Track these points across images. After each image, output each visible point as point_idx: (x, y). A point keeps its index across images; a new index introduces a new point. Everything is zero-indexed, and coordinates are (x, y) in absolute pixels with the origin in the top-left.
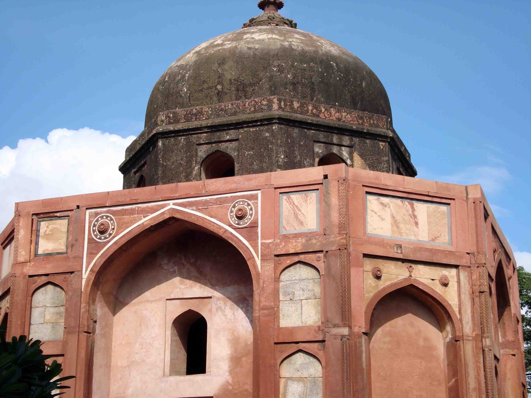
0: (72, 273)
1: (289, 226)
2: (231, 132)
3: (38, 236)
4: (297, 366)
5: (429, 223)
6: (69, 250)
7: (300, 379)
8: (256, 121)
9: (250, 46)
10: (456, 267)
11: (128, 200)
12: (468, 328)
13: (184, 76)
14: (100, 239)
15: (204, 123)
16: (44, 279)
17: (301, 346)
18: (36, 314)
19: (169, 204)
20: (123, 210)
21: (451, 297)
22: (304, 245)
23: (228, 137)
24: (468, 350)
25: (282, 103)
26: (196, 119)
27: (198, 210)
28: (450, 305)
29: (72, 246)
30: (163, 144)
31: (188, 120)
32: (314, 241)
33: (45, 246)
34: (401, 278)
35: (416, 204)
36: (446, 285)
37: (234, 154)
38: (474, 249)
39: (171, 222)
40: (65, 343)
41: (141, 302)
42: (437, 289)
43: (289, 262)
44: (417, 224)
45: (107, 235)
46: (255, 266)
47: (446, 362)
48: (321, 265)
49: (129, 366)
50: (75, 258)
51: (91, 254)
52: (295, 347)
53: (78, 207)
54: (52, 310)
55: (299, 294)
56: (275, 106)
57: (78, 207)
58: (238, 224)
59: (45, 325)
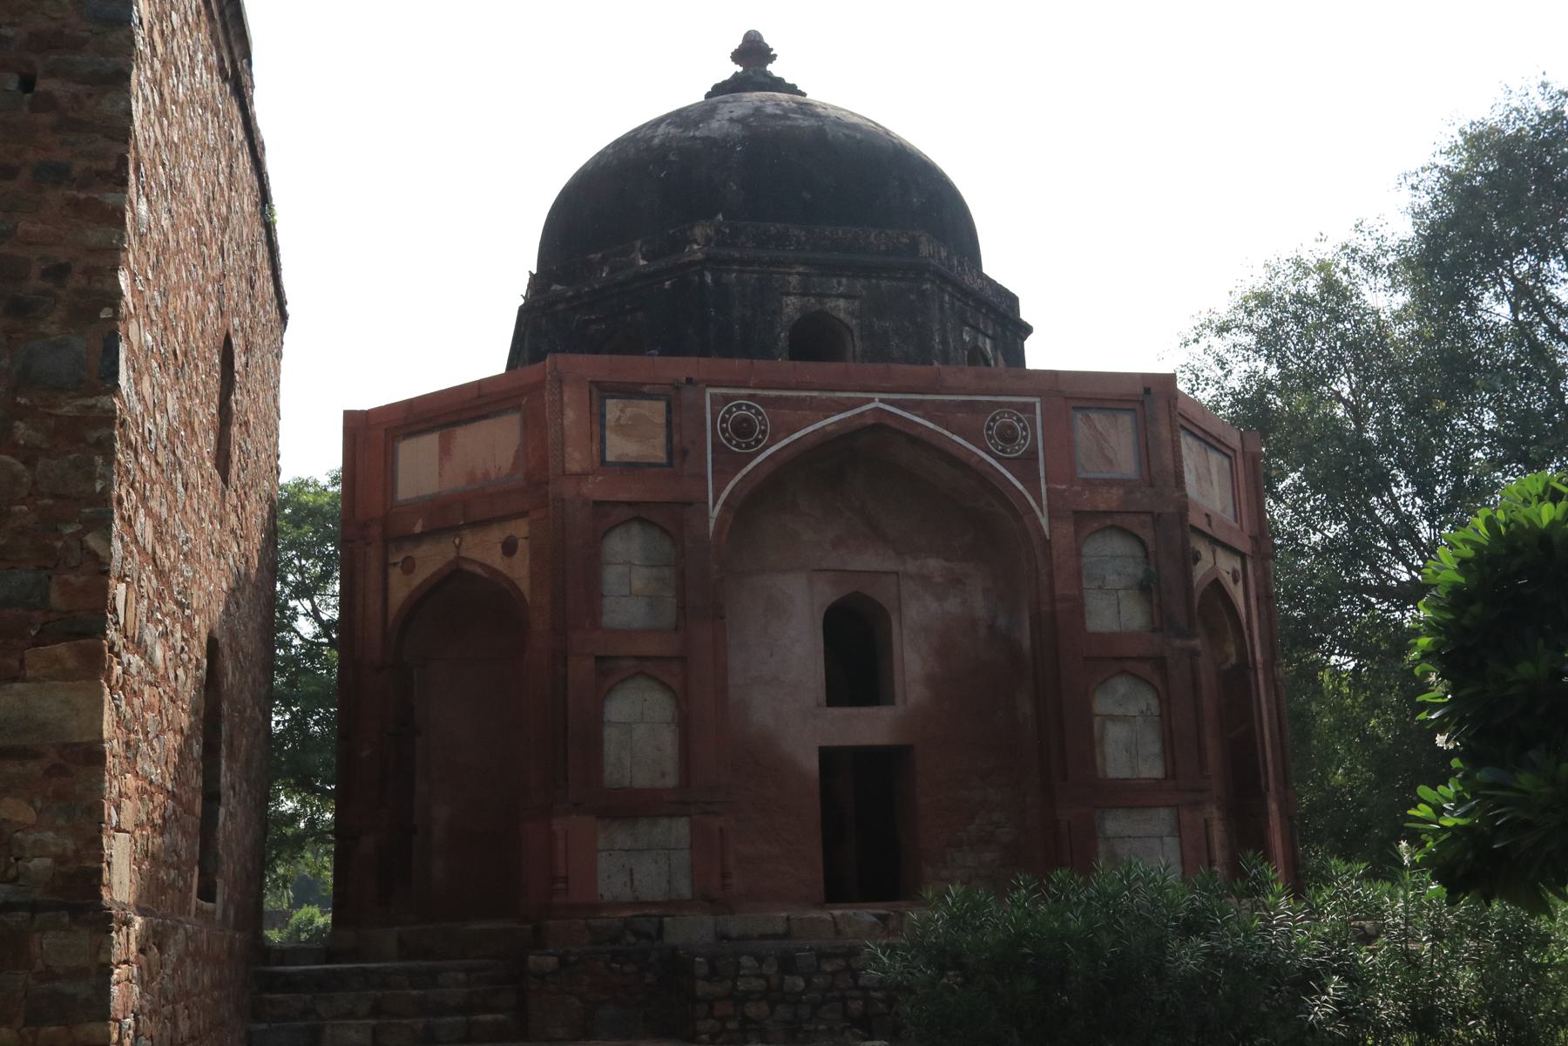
0: (690, 504)
1: (1090, 467)
3: (603, 426)
7: (1124, 719)
18: (612, 577)
19: (872, 400)
29: (685, 453)
33: (619, 447)
39: (880, 429)
46: (1040, 528)
48: (1147, 535)
51: (722, 475)
53: (689, 380)
57: (689, 380)
58: (1003, 451)
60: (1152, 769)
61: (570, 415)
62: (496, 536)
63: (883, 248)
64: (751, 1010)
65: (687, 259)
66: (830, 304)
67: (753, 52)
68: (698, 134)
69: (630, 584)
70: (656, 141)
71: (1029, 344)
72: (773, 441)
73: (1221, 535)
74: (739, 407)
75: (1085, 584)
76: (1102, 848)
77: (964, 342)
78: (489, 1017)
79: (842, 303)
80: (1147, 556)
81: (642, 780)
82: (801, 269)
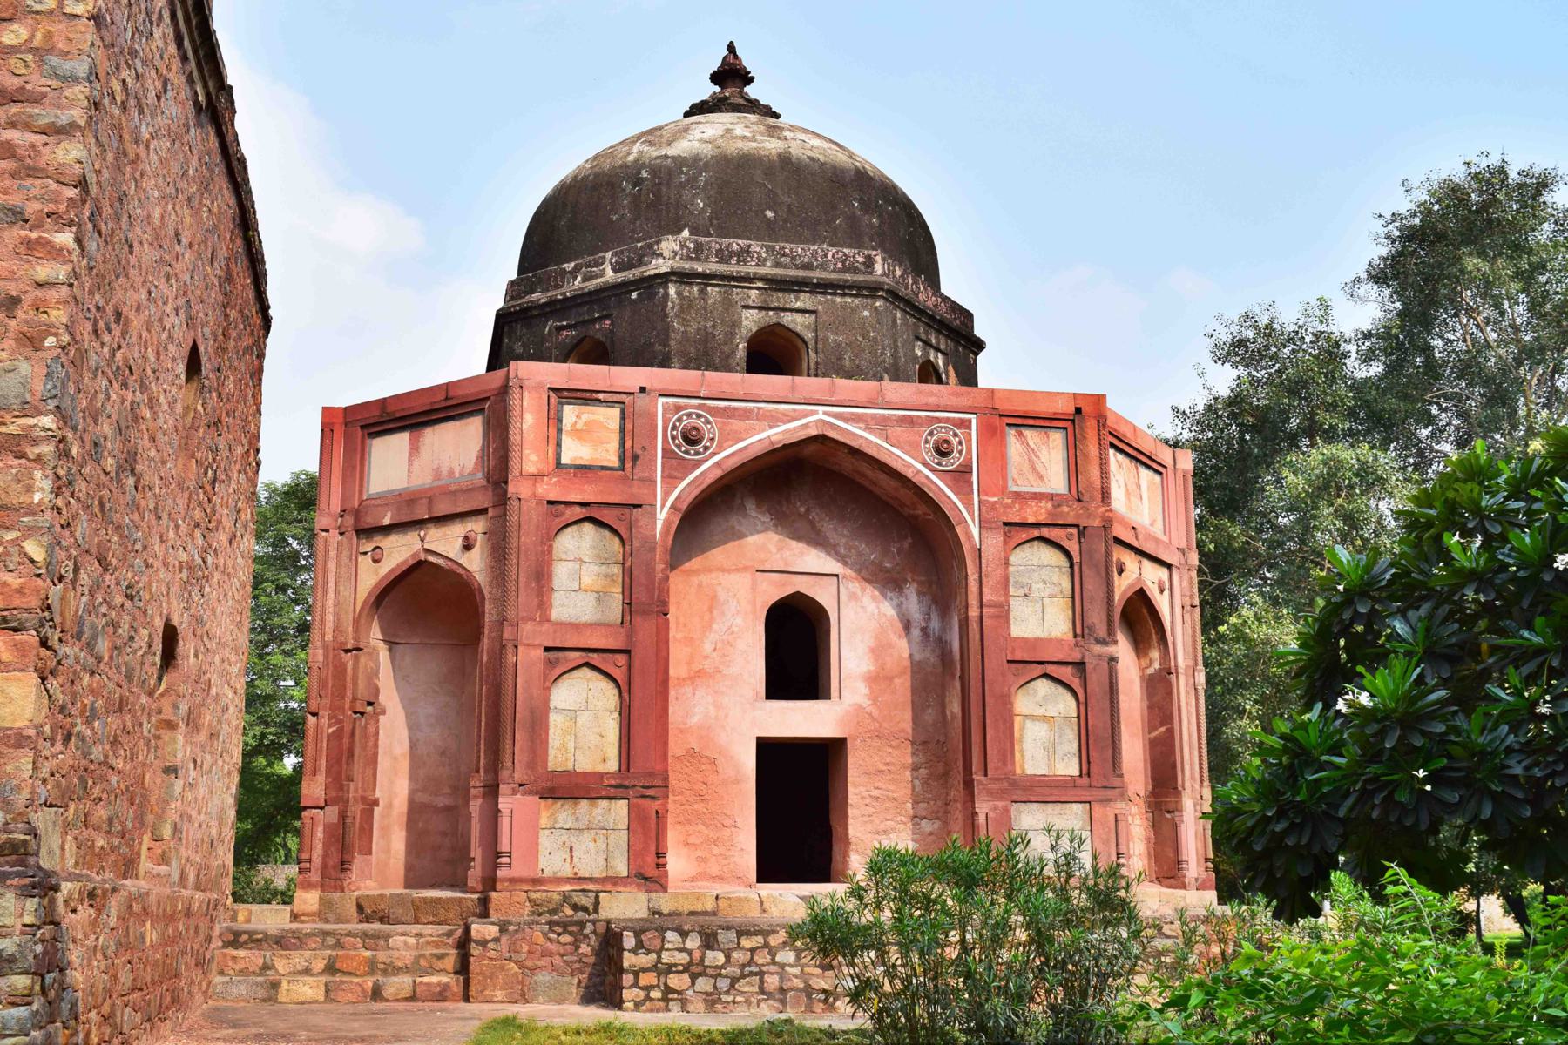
2: (802, 296)
3: (560, 431)
4: (1039, 698)
6: (628, 465)
7: (1044, 719)
9: (815, 155)
10: (1169, 566)
11: (741, 394)
13: (692, 180)
14: (687, 452)
15: (762, 271)
16: (579, 512)
17: (1050, 669)
18: (562, 574)
19: (816, 412)
20: (729, 408)
22: (1049, 513)
23: (798, 305)
26: (738, 262)
27: (868, 429)
29: (635, 458)
30: (679, 293)
31: (724, 260)
32: (1066, 509)
33: (573, 451)
36: (1162, 591)
37: (809, 336)
43: (1024, 536)
45: (700, 448)
46: (969, 536)
47: (1146, 703)
48: (1073, 547)
49: (690, 678)
50: (642, 480)
51: (671, 479)
52: (1039, 670)
54: (595, 568)
55: (1037, 588)
56: (879, 268)
57: (643, 389)
59: (581, 595)
60: (1069, 767)
61: (529, 419)
62: (457, 531)
63: (840, 265)
64: (675, 981)
65: (652, 272)
67: (731, 74)
68: (670, 153)
69: (579, 581)
70: (631, 158)
71: (982, 359)
72: (721, 448)
73: (1149, 548)
74: (689, 416)
75: (1012, 591)
77: (916, 357)
78: (434, 979)
79: (799, 317)
80: (1072, 566)
81: (585, 764)
82: (760, 284)
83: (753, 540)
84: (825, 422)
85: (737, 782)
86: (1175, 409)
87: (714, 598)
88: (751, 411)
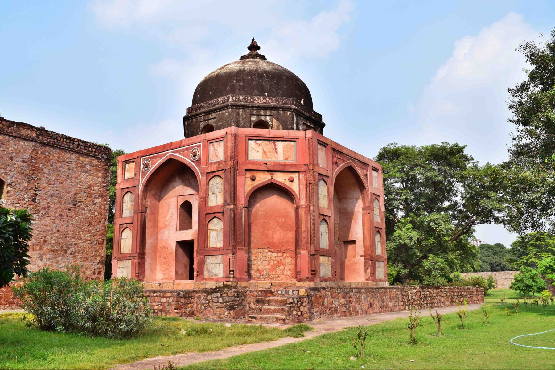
1: (212, 160)
2: (213, 114)
5: (284, 151)
7: (215, 230)
8: (222, 108)
10: (298, 172)
12: (303, 202)
16: (126, 190)
21: (295, 187)
22: (217, 167)
23: (212, 117)
24: (302, 212)
25: (234, 98)
28: (294, 191)
33: (128, 175)
34: (266, 179)
35: (277, 142)
38: (307, 163)
40: (133, 217)
41: (168, 198)
42: (287, 183)
43: (212, 176)
44: (277, 152)
48: (223, 176)
51: (143, 177)
52: (213, 216)
55: (216, 191)
56: (230, 100)
60: (220, 245)
66: (210, 121)
67: (254, 47)
76: (205, 267)
79: (212, 121)
83: (178, 188)
84: (171, 155)
85: (172, 253)
86: (509, 90)
87: (169, 205)
88: (157, 156)
